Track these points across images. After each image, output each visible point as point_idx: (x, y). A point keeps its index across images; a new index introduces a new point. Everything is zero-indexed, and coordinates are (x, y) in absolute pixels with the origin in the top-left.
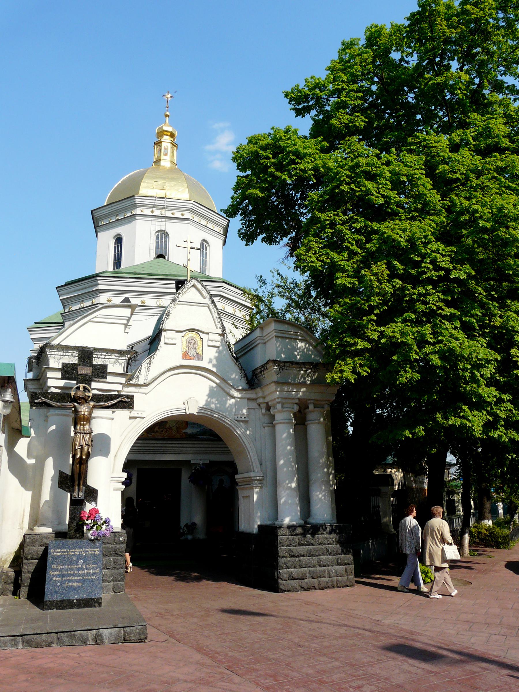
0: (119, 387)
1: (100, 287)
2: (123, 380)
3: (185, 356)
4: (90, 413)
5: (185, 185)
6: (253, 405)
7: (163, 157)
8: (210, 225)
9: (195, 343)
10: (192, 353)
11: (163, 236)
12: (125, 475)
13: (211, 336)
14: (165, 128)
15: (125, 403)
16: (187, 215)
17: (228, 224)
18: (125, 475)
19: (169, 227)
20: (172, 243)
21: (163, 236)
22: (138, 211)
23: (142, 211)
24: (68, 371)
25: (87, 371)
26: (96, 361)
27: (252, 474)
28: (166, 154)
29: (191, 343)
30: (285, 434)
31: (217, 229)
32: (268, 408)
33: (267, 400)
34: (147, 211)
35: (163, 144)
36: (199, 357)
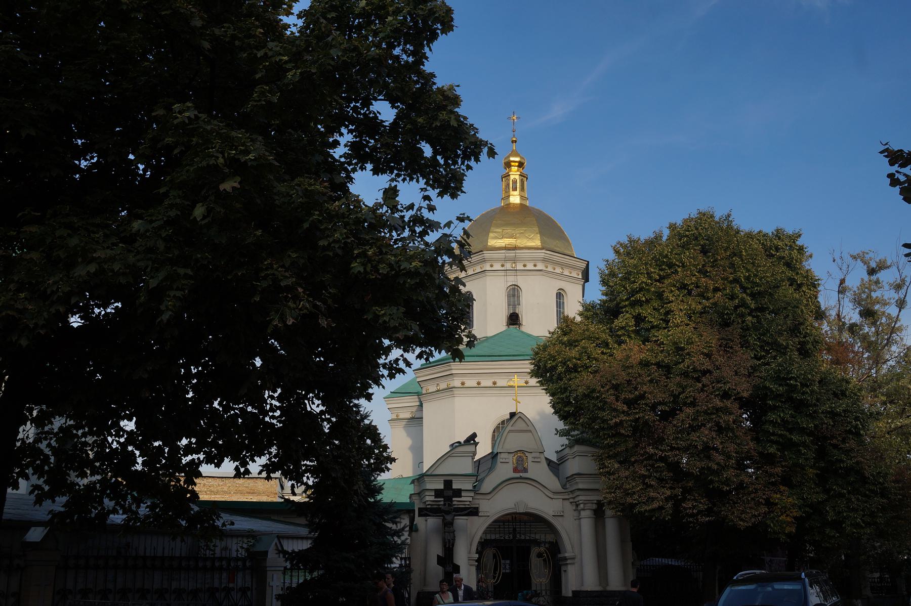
0: (470, 499)
1: (454, 372)
2: (472, 494)
3: (515, 470)
4: (453, 519)
5: (537, 229)
6: (567, 503)
7: (512, 192)
8: (566, 272)
9: (523, 460)
10: (520, 468)
11: (514, 293)
12: (477, 556)
13: (534, 455)
14: (512, 159)
15: (473, 512)
16: (540, 266)
17: (588, 265)
18: (477, 556)
19: (522, 281)
21: (514, 293)
22: (488, 268)
23: (492, 266)
24: (438, 493)
25: (450, 493)
26: (454, 487)
27: (566, 555)
28: (515, 189)
29: (520, 460)
30: (587, 525)
31: (574, 274)
32: (577, 506)
33: (576, 500)
34: (497, 266)
35: (512, 177)
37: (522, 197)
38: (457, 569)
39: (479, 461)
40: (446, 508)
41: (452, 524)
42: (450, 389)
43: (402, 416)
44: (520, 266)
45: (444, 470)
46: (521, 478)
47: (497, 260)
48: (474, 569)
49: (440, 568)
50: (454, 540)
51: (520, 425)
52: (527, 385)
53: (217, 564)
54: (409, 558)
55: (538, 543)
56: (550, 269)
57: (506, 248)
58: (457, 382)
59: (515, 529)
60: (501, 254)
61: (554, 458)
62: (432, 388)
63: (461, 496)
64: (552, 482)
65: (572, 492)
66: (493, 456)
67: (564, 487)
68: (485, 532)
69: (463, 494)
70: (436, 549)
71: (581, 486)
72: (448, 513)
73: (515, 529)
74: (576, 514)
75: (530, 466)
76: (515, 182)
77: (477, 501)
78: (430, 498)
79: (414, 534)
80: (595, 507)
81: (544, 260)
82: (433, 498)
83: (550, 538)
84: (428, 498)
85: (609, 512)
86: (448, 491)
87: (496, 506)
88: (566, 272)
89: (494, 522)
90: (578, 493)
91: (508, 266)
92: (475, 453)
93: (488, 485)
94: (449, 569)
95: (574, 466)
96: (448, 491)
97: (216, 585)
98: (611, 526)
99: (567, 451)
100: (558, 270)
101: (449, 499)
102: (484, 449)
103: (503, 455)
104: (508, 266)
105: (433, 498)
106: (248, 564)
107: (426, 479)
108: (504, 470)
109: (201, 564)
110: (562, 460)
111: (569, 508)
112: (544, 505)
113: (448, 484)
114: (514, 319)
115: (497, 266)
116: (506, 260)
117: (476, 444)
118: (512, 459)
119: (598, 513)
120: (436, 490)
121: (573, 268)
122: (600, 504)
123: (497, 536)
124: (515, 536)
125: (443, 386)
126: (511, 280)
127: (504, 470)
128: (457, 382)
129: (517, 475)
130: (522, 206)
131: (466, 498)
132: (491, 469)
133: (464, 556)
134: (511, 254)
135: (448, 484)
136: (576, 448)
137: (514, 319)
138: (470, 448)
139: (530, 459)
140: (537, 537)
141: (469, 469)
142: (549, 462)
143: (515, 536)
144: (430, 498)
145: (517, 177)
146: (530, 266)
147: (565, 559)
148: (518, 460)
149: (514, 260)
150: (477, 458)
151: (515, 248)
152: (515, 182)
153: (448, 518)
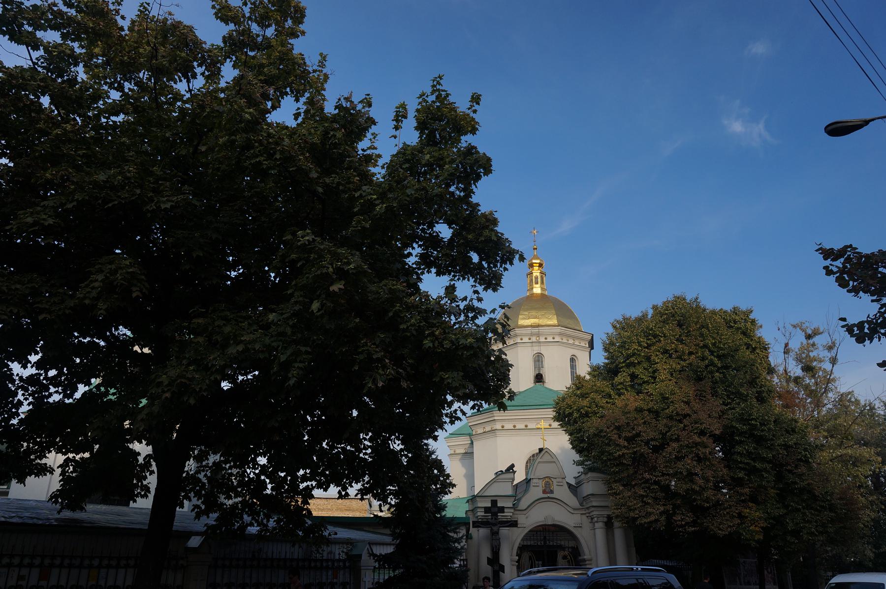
3: (544, 492)
5: (554, 312)
6: (584, 517)
8: (577, 343)
11: (539, 359)
15: (514, 524)
16: (557, 339)
19: (544, 350)
20: (547, 363)
21: (539, 359)
22: (519, 341)
24: (487, 510)
25: (496, 510)
28: (537, 283)
30: (600, 533)
31: (583, 344)
34: (526, 340)
35: (534, 274)
36: (552, 492)
37: (542, 289)
38: (502, 568)
39: (517, 485)
40: (493, 521)
41: (497, 533)
42: (493, 431)
43: (458, 451)
44: (542, 339)
45: (492, 492)
46: (549, 498)
47: (525, 335)
48: (515, 568)
49: (489, 567)
50: (499, 545)
51: (547, 458)
52: (550, 427)
53: (324, 564)
54: (466, 560)
55: (562, 548)
56: (565, 340)
57: (531, 326)
58: (498, 426)
59: (545, 537)
60: (529, 331)
61: (573, 482)
62: (480, 431)
63: (503, 512)
64: (573, 501)
65: (588, 508)
66: (527, 481)
67: (581, 504)
68: (523, 540)
69: (506, 510)
70: (486, 553)
71: (594, 504)
72: (495, 525)
73: (545, 537)
74: (591, 525)
75: (555, 488)
76: (536, 278)
77: (516, 516)
78: (481, 513)
79: (469, 541)
80: (605, 520)
81: (560, 334)
82: (483, 514)
83: (572, 544)
84: (479, 514)
85: (617, 524)
86: (494, 509)
87: (532, 519)
88: (577, 343)
89: (530, 531)
90: (592, 509)
91: (534, 339)
92: (513, 480)
93: (523, 504)
94: (497, 568)
95: (589, 488)
96: (494, 509)
97: (324, 580)
98: (618, 534)
99: (583, 476)
100: (571, 341)
101: (495, 515)
102: (520, 476)
103: (534, 481)
104: (534, 339)
105: (483, 514)
106: (347, 564)
107: (478, 499)
108: (536, 492)
109: (313, 564)
110: (579, 484)
111: (586, 521)
112: (567, 519)
113: (494, 503)
114: (539, 378)
115: (526, 340)
116: (532, 334)
117: (514, 472)
118: (541, 484)
119: (609, 524)
120: (485, 508)
121: (582, 339)
122: (609, 518)
123: (532, 543)
124: (545, 543)
125: (488, 429)
126: (536, 349)
127: (536, 492)
128: (498, 426)
129: (546, 496)
130: (542, 295)
131: (508, 514)
132: (526, 491)
133: (507, 557)
134: (535, 330)
135: (494, 503)
136: (590, 475)
137: (539, 378)
138: (510, 476)
139: (555, 483)
140: (563, 543)
141: (510, 492)
142: (570, 485)
143: (545, 543)
144: (481, 513)
145: (538, 274)
146: (550, 339)
147: (585, 560)
148: (546, 484)
149: (538, 335)
150: (515, 483)
151: (538, 326)
152: (536, 278)
153: (495, 528)
